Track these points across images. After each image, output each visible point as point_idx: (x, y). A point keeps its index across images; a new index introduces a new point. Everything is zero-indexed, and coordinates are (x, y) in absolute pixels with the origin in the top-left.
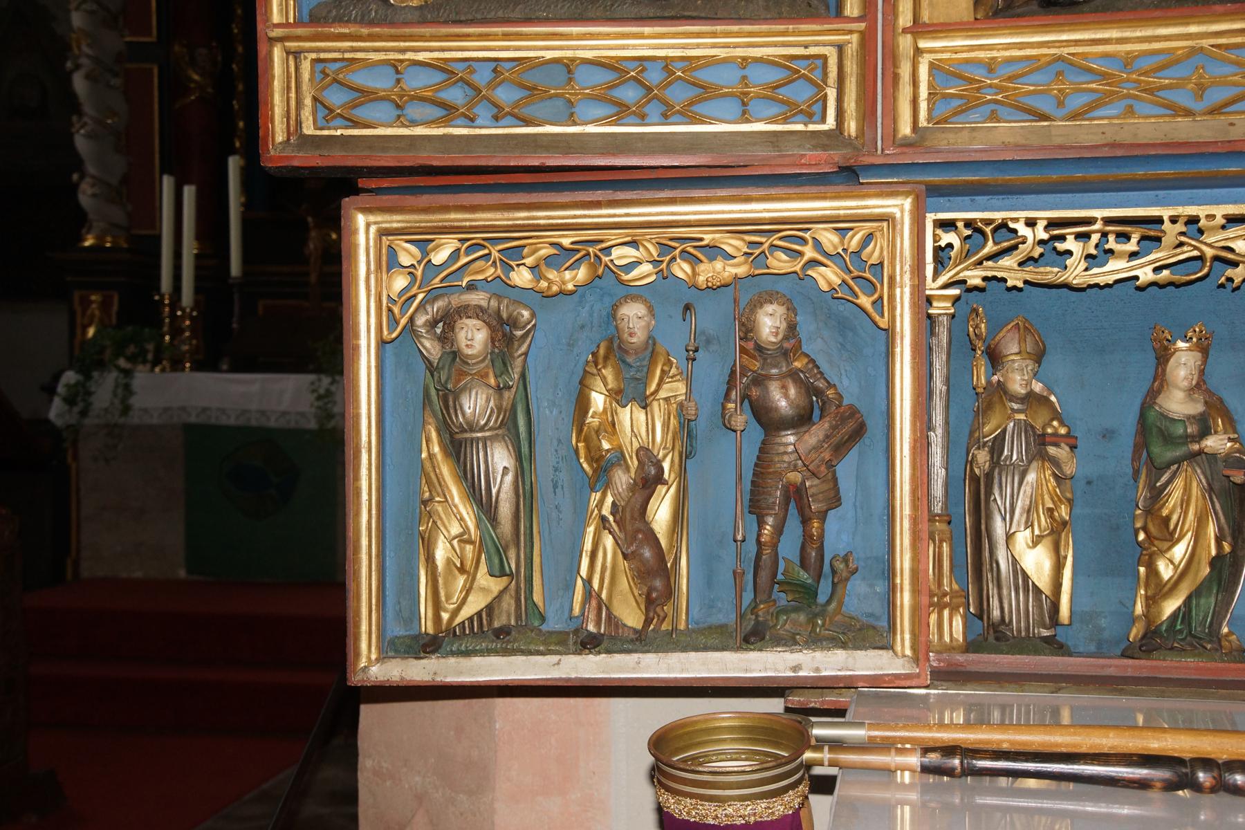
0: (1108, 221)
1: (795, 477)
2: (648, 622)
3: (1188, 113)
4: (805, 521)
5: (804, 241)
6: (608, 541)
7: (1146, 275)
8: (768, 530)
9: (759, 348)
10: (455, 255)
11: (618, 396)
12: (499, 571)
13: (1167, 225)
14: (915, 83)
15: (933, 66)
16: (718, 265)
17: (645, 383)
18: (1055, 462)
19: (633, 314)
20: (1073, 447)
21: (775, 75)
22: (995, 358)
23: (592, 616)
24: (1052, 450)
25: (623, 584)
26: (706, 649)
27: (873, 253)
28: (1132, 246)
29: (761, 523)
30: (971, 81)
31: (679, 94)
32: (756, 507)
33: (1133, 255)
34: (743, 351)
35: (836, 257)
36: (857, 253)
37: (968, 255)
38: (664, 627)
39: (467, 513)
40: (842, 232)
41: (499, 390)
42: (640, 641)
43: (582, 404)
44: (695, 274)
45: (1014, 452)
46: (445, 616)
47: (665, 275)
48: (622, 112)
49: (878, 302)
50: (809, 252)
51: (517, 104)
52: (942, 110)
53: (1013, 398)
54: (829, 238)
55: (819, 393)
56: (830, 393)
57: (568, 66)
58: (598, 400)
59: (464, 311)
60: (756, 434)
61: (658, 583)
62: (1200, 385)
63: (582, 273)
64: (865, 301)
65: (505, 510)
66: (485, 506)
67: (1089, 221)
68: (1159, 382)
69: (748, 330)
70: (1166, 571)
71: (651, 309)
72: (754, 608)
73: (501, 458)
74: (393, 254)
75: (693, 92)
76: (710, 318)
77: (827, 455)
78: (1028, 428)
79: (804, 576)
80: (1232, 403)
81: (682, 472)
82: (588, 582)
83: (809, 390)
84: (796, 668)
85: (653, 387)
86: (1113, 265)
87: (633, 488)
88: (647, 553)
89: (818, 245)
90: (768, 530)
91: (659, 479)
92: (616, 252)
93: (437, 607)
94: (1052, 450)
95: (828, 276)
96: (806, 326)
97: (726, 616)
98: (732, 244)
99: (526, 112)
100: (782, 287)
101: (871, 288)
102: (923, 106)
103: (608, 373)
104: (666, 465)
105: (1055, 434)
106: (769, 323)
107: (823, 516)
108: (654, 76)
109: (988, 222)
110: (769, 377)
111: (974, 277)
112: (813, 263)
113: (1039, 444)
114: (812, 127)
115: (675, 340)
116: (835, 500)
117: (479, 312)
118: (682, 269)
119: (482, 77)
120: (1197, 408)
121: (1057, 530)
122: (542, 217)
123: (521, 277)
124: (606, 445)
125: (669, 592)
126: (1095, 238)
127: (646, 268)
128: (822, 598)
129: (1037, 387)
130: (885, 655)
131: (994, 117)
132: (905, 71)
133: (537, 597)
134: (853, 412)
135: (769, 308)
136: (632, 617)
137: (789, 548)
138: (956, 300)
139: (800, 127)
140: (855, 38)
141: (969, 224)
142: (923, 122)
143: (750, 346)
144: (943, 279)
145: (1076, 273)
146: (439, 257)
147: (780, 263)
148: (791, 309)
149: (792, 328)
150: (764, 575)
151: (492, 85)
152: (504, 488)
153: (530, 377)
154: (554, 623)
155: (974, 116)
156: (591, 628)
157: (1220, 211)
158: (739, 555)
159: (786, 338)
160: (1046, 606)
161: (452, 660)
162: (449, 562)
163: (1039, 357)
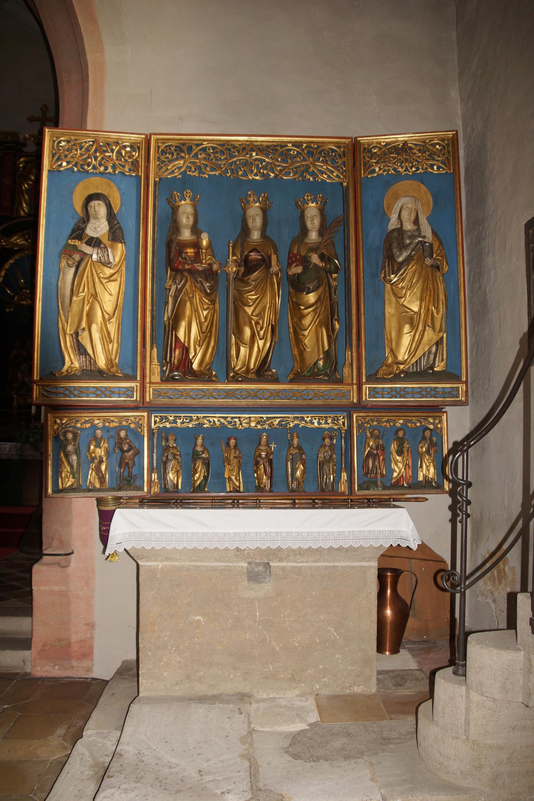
0: (184, 416)
1: (127, 461)
2: (101, 487)
3: (195, 399)
4: (129, 468)
5: (129, 420)
6: (94, 473)
7: (190, 426)
8: (122, 470)
9: (121, 438)
10: (67, 422)
11: (96, 447)
12: (74, 477)
13: (193, 417)
14: (150, 392)
15: (153, 389)
16: (114, 423)
17: (100, 444)
18: (177, 459)
19: (99, 432)
20: (180, 457)
21: (125, 390)
22: (167, 440)
23: (90, 486)
24: (176, 457)
25: (96, 480)
26: (111, 491)
27: (140, 422)
28: (188, 421)
29: (121, 469)
30: (159, 392)
31: (108, 393)
32: (120, 466)
33: (188, 423)
34: (118, 439)
35: (134, 423)
36: (138, 422)
37: (160, 422)
38: (104, 488)
39: (68, 468)
40: (135, 418)
41: (74, 445)
42: (99, 490)
43: (89, 448)
44: (109, 425)
45: (170, 457)
46: (64, 486)
47: (104, 425)
48: (98, 396)
49: (142, 431)
50: (130, 422)
51: (78, 394)
52: (155, 396)
53: (170, 447)
54: (133, 419)
55: (131, 446)
56: (133, 446)
57: (88, 388)
58: (92, 447)
59: (68, 431)
60: (121, 453)
61: (103, 480)
62: (202, 445)
63: (89, 425)
64: (139, 430)
65: (75, 467)
66: (72, 466)
67: (181, 416)
68: (196, 445)
69: (119, 435)
70: (196, 479)
71: (102, 431)
72: (120, 484)
73: (74, 458)
74: (55, 421)
75: (110, 392)
76: (112, 433)
77: (132, 457)
78: (173, 453)
79: (129, 479)
80: (208, 448)
81: (107, 460)
82: (90, 480)
83: (130, 446)
84: (127, 494)
85: (102, 445)
86: (185, 424)
87: (98, 463)
88: (101, 475)
89: (131, 420)
90: (122, 470)
91: (103, 461)
92: (95, 421)
93: (63, 484)
94: (176, 457)
95: (132, 426)
96: (129, 434)
97: (115, 486)
98: (116, 420)
99: (80, 396)
100: (125, 428)
101: (140, 428)
102: (151, 396)
103: (94, 442)
104: (104, 459)
105: (177, 454)
106: (123, 434)
107: (132, 467)
108: (103, 389)
109: (164, 416)
110: (122, 443)
111: (161, 426)
112: (131, 423)
113: (174, 455)
114: (132, 399)
115: (106, 436)
116: (134, 465)
117: (71, 431)
118: (107, 424)
119: (72, 389)
120: (202, 449)
121: (177, 472)
122: (83, 415)
123: (79, 425)
124: (93, 455)
125: (104, 481)
126: (182, 419)
127: (101, 424)
128: (132, 482)
129: (174, 445)
130: (142, 492)
131: (163, 398)
132: (148, 390)
133: (81, 483)
134: (138, 450)
135: (123, 431)
136: (98, 486)
137: (126, 474)
138: (158, 429)
139: (129, 399)
140: (139, 384)
141: (160, 416)
142: (151, 398)
143: (119, 438)
144: (156, 426)
145: (179, 425)
146: (64, 422)
147: (124, 423)
148: (126, 431)
149: (127, 435)
150: (122, 478)
151: (74, 391)
152: (75, 463)
153: (80, 443)
154: (84, 488)
155: (160, 398)
156: (90, 488)
157: (202, 415)
158: (117, 475)
159: (126, 436)
160: (175, 485)
161: (65, 494)
162: (65, 476)
163: (175, 440)
